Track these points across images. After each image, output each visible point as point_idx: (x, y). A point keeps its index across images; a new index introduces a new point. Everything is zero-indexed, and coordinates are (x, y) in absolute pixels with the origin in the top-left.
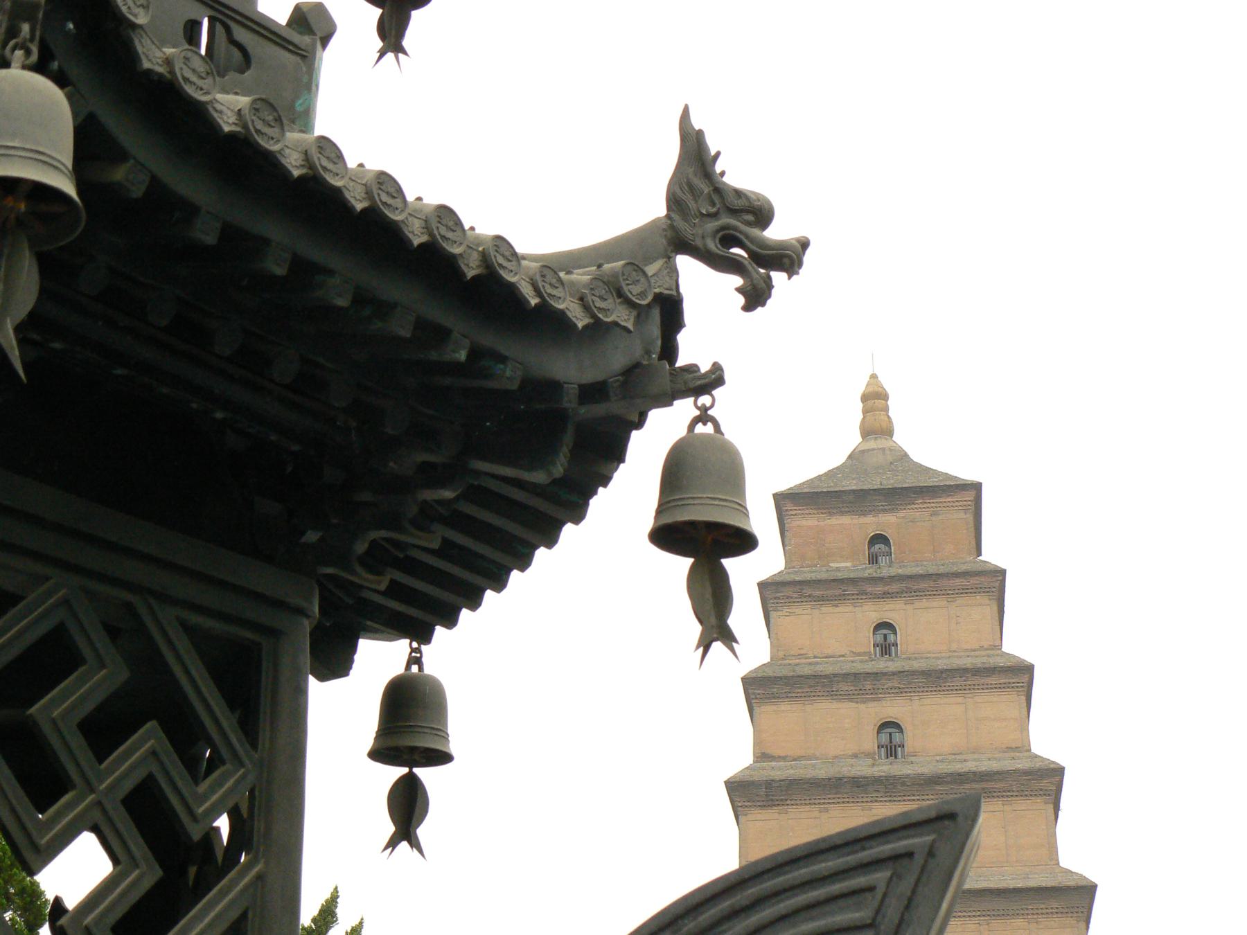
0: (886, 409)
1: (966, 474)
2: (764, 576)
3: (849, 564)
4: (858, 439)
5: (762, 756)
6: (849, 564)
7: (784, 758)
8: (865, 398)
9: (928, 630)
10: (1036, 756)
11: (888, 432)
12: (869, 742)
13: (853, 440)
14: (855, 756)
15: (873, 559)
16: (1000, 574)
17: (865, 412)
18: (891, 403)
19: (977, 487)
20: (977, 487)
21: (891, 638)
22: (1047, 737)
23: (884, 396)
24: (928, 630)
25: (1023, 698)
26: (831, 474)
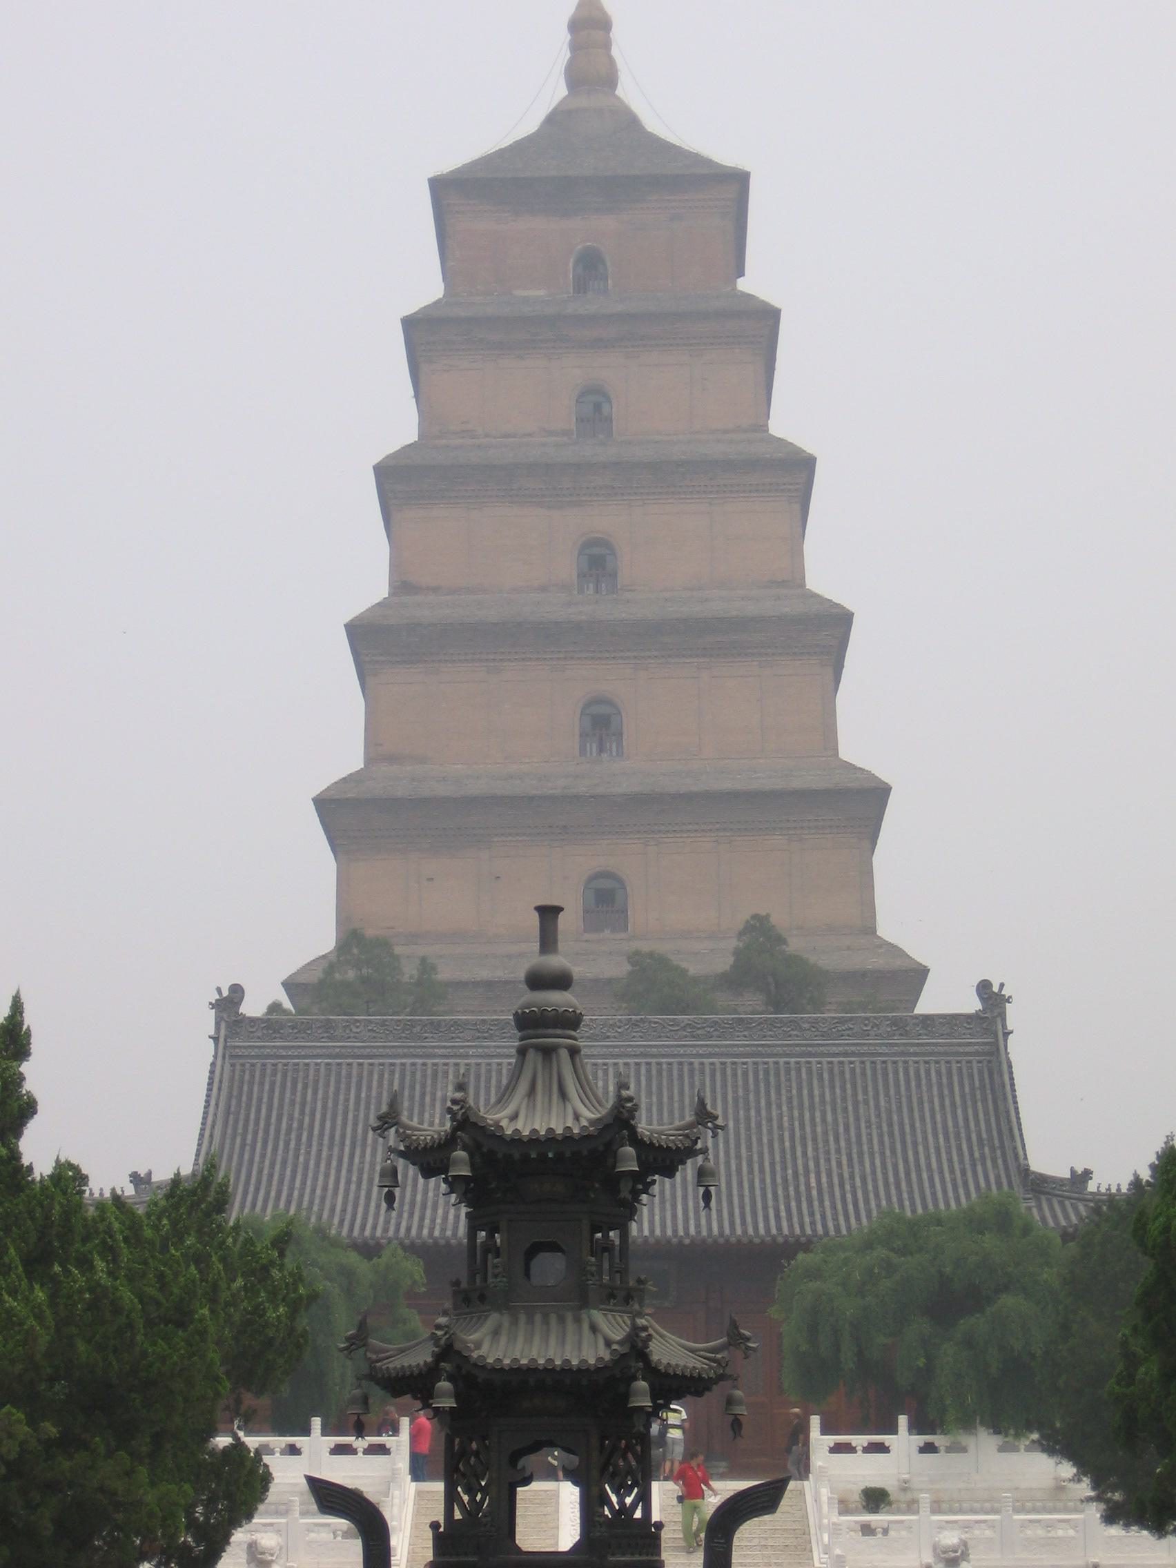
0: (607, 45)
1: (725, 155)
2: (411, 308)
3: (541, 293)
4: (563, 91)
5: (401, 585)
6: (541, 293)
7: (435, 590)
8: (575, 26)
9: (658, 400)
10: (815, 596)
11: (609, 80)
12: (566, 567)
13: (554, 92)
14: (543, 589)
15: (581, 287)
16: (769, 317)
17: (575, 47)
18: (616, 33)
19: (740, 180)
20: (740, 180)
21: (606, 408)
22: (827, 571)
23: (604, 24)
24: (658, 400)
25: (797, 507)
26: (519, 148)
